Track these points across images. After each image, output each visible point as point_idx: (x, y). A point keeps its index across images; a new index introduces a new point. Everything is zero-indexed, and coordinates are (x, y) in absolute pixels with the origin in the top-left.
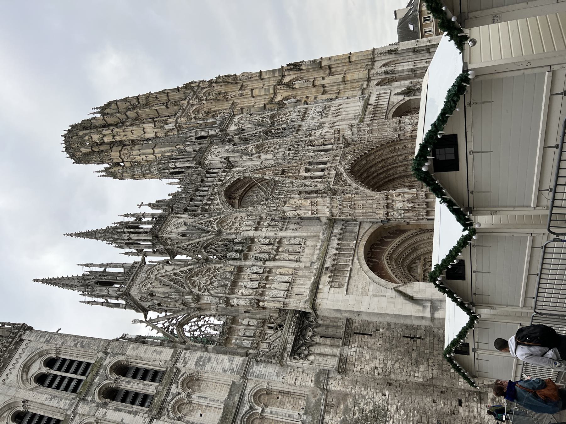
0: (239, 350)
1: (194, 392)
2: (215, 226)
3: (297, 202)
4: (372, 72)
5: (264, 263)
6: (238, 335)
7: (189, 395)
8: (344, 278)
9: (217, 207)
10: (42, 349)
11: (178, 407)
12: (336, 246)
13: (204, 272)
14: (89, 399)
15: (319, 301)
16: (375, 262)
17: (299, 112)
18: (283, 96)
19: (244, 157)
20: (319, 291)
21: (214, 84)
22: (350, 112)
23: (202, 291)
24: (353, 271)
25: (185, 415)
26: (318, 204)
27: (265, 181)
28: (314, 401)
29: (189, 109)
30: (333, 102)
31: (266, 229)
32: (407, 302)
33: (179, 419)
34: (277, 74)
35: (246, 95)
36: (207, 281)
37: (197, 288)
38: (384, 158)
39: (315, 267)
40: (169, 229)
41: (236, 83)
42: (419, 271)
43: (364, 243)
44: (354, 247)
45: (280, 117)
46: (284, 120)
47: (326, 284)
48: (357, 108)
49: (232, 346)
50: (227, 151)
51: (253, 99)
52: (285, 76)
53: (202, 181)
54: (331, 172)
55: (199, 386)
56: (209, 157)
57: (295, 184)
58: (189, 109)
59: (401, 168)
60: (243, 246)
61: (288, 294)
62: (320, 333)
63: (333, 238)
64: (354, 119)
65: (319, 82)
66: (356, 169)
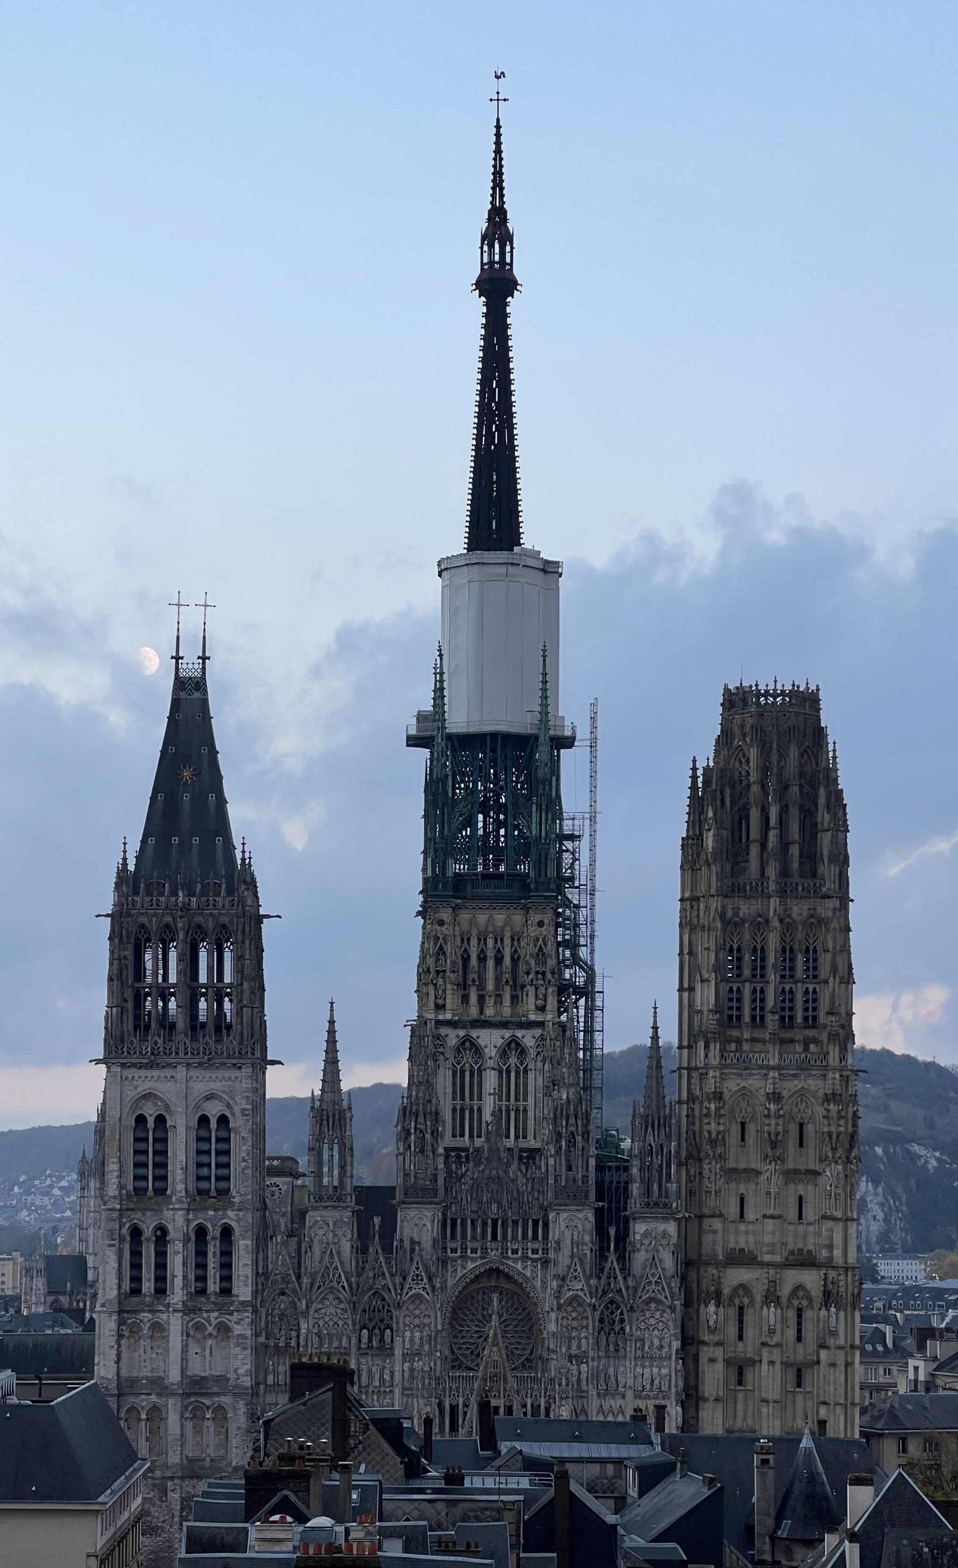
0: (262, 1374)
1: (216, 1337)
2: (413, 1291)
6: (279, 1364)
7: (210, 1335)
10: (235, 1107)
11: (199, 1327)
13: (342, 1306)
14: (191, 1216)
25: (194, 1337)
28: (223, 1466)
29: (754, 1074)
33: (188, 1335)
34: (825, 1253)
37: (320, 1306)
41: (821, 1161)
55: (222, 1340)
56: (564, 1215)
58: (754, 1074)
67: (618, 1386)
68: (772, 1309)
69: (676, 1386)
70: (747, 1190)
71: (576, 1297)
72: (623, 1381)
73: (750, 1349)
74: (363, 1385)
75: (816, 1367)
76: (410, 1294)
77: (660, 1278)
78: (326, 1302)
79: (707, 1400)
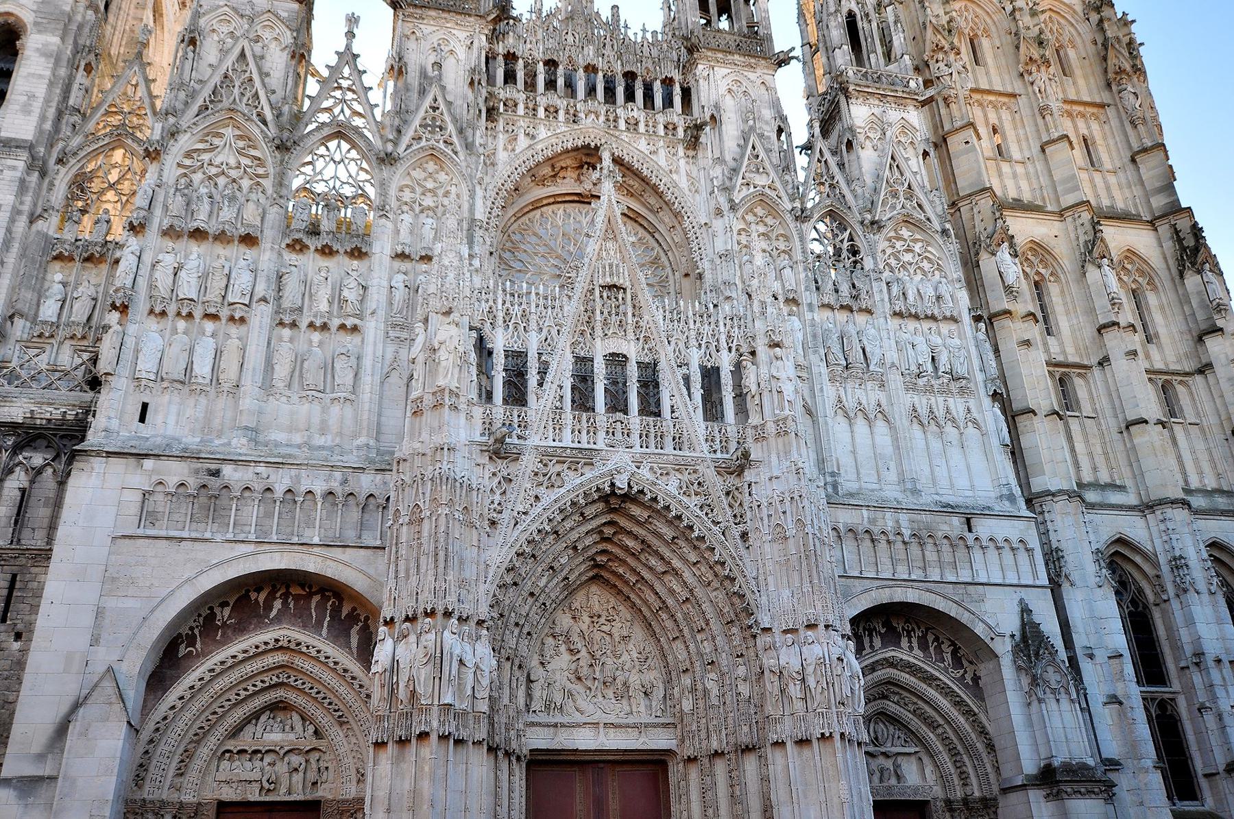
3: (443, 347)
4: (1179, 515)
5: (264, 300)
8: (180, 525)
9: (521, 137)
12: (303, 489)
15: (95, 466)
16: (268, 607)
17: (939, 298)
18: (1052, 243)
19: (717, 172)
20: (132, 460)
21: (1094, 17)
22: (936, 461)
23: (188, 162)
24: (197, 545)
26: (436, 413)
27: (662, 254)
30: (987, 402)
31: (401, 286)
32: (64, 708)
34: (1159, 202)
35: (1046, 125)
36: (217, 166)
37: (200, 146)
38: (699, 592)
39: (234, 441)
40: (427, 29)
41: (1109, 85)
42: (275, 737)
43: (310, 563)
44: (295, 540)
45: (917, 247)
46: (898, 259)
47: (155, 478)
48: (962, 482)
49: (49, 277)
50: (749, 114)
51: (1036, 149)
52: (1156, 230)
53: (630, 76)
54: (601, 435)
56: (721, 71)
57: (554, 332)
59: (685, 654)
60: (328, 233)
61: (144, 382)
62: (36, 485)
63: (338, 475)
64: (902, 481)
65: (1116, 343)
66: (636, 511)
67: (868, 366)
68: (1107, 268)
69: (983, 370)
70: (1000, 118)
71: (762, 199)
72: (877, 351)
73: (1070, 350)
74: (286, 304)
75: (1199, 379)
76: (414, 148)
77: (909, 187)
78: (216, 141)
79: (1033, 412)
